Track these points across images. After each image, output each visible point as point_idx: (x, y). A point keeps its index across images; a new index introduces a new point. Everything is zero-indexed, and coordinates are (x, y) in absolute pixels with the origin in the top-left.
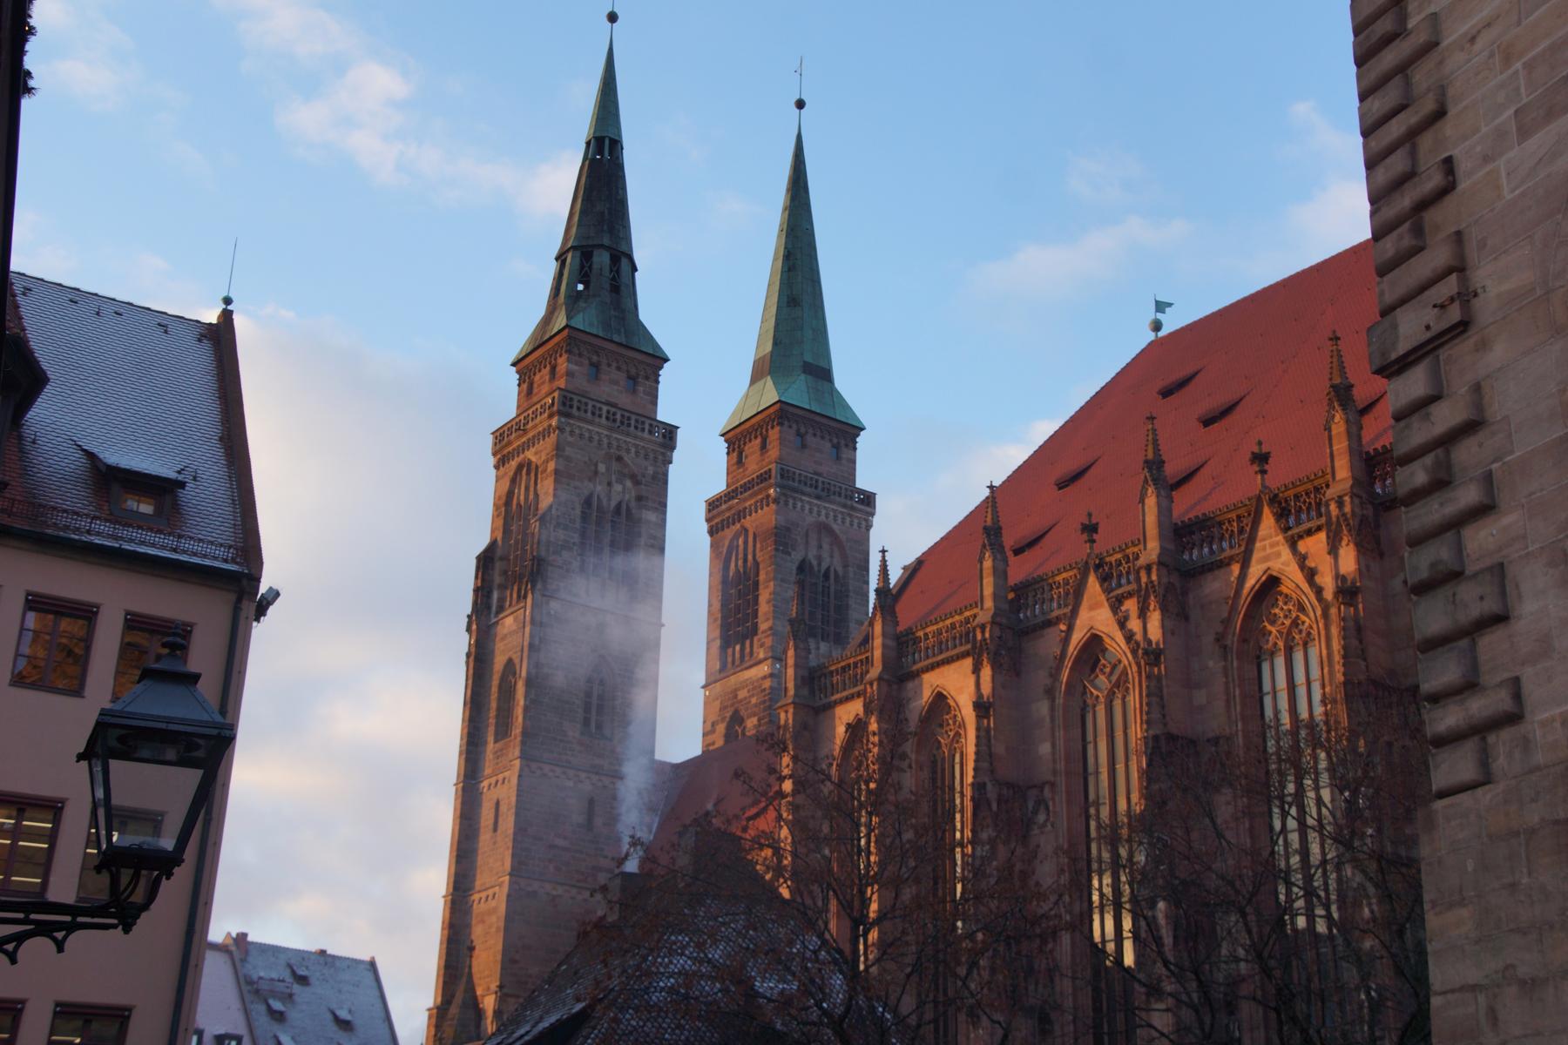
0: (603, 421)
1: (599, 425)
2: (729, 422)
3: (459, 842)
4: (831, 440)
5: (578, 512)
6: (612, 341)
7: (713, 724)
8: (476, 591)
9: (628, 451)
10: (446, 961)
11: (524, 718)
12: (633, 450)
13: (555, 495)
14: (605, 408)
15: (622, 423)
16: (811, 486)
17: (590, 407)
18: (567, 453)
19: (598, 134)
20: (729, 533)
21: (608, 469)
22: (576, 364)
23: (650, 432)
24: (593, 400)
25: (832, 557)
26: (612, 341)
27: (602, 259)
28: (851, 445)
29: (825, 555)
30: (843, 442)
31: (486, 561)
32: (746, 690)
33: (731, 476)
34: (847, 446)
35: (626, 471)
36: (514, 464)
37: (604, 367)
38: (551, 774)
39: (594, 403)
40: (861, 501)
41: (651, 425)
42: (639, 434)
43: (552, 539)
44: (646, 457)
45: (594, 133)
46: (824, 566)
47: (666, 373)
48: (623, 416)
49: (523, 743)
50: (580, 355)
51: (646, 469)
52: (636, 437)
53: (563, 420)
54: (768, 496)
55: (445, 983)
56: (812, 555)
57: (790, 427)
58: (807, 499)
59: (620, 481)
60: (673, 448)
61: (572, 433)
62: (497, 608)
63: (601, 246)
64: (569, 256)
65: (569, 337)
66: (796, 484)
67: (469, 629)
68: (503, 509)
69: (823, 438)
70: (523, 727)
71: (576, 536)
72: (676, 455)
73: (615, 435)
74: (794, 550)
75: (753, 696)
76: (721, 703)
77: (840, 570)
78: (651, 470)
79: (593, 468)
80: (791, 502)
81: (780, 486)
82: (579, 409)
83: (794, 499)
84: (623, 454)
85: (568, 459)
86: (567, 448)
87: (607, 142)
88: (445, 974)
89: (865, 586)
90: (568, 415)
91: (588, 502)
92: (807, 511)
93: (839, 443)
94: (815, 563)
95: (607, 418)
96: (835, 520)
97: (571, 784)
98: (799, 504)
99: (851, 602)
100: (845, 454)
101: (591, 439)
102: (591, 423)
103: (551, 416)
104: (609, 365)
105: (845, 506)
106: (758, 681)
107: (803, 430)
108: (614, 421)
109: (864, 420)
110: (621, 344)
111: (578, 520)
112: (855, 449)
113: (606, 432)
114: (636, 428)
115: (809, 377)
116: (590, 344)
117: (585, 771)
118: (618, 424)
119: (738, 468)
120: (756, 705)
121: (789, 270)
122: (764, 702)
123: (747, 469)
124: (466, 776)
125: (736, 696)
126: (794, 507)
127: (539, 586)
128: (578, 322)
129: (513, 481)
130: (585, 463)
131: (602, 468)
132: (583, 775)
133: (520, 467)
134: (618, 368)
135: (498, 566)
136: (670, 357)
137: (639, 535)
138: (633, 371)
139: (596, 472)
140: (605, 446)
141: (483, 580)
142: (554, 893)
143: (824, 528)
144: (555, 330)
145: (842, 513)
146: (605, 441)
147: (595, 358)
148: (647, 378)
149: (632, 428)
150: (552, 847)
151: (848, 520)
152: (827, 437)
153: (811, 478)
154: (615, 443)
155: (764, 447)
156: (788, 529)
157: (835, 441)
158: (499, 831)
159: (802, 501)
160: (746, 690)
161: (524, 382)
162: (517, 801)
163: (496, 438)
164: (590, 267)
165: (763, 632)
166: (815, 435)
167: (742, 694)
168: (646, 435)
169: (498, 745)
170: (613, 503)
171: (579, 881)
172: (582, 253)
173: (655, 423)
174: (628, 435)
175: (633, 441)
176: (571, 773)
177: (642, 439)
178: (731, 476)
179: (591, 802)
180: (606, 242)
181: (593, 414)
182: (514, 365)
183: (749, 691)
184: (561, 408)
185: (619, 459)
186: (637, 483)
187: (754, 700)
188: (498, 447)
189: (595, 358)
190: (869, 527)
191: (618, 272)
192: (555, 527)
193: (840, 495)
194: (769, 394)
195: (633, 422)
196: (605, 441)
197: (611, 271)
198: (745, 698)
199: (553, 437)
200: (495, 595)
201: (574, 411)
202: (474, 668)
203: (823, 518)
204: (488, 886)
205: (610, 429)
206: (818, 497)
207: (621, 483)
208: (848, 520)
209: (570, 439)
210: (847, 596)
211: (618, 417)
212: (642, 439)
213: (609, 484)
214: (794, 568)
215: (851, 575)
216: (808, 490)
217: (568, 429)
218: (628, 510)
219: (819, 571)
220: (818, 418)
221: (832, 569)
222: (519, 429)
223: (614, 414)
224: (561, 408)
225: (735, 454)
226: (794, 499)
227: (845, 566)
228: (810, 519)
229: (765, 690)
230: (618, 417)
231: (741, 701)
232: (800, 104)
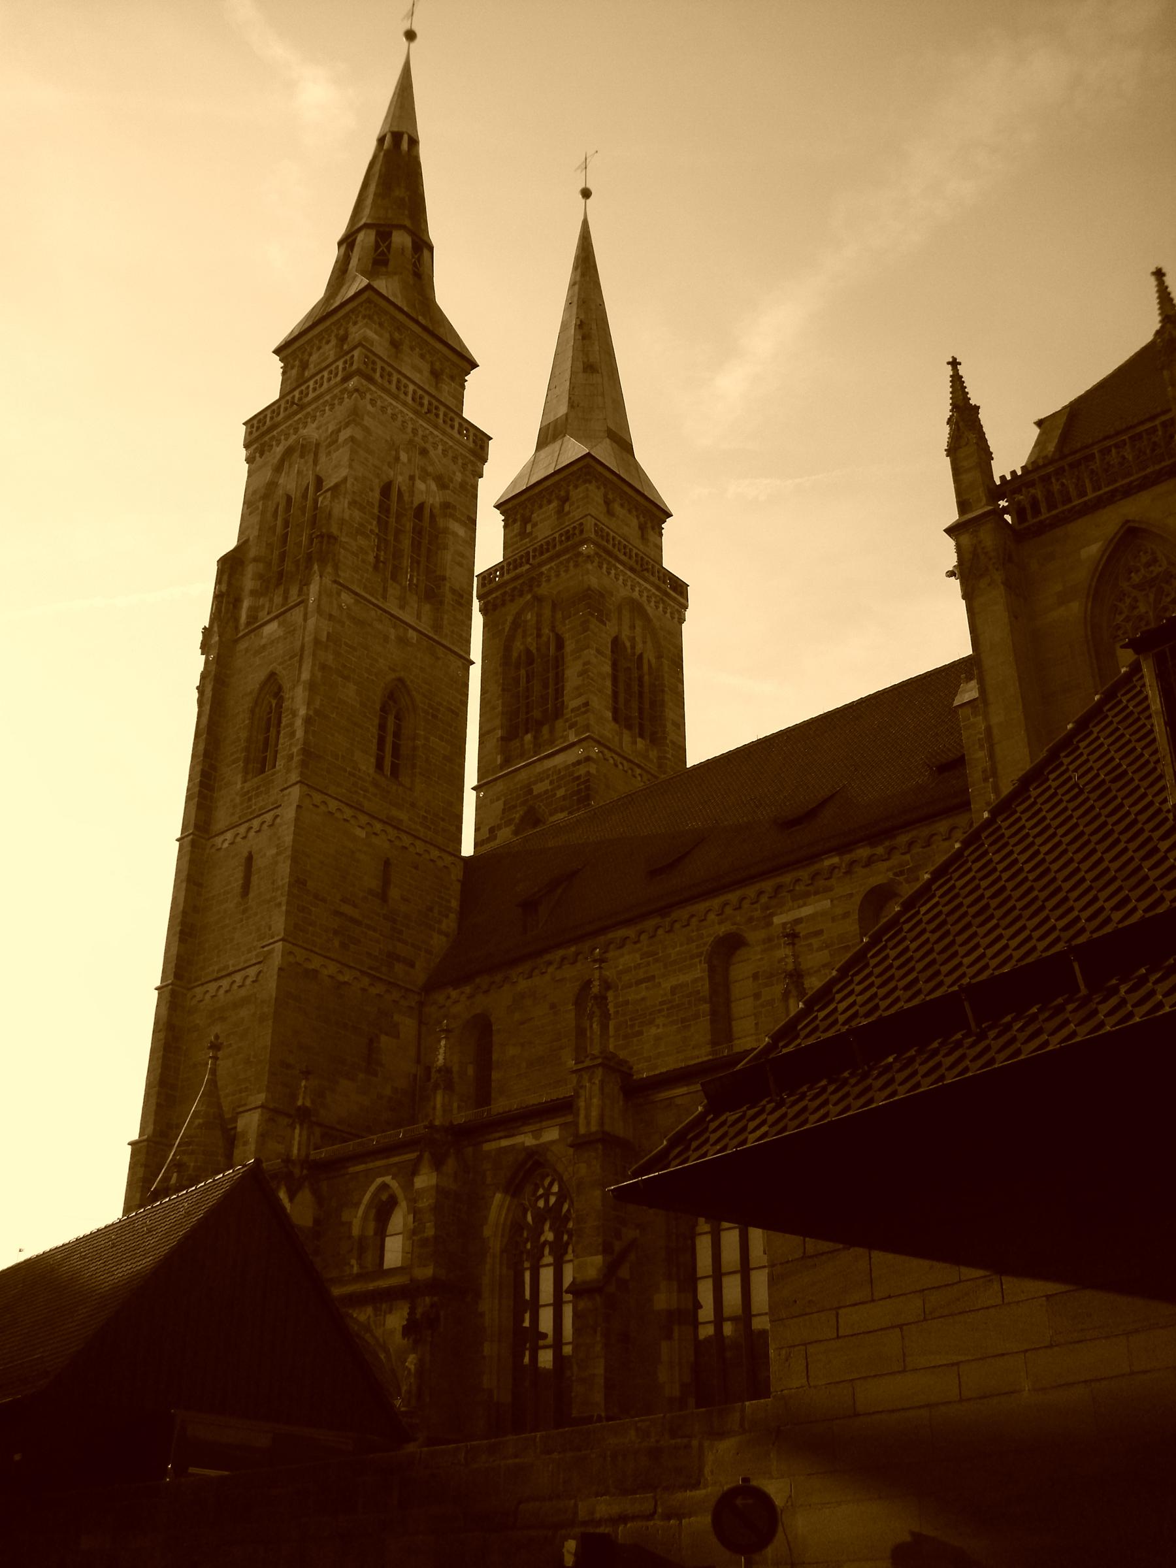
0: (409, 399)
1: (405, 404)
2: (514, 483)
3: (185, 913)
4: (638, 517)
5: (377, 495)
6: (417, 322)
7: (492, 830)
8: (218, 597)
9: (435, 448)
10: (162, 1074)
11: (306, 732)
12: (440, 447)
13: (350, 466)
14: (411, 387)
15: (429, 411)
16: (625, 554)
17: (394, 379)
18: (365, 423)
20: (512, 609)
21: (409, 460)
22: (376, 333)
23: (460, 433)
24: (399, 372)
25: (644, 643)
26: (417, 322)
27: (401, 239)
28: (657, 530)
29: (638, 639)
30: (649, 525)
31: (229, 566)
32: (547, 782)
33: (510, 550)
34: (653, 529)
35: (430, 469)
36: (279, 450)
37: (405, 348)
38: (338, 815)
39: (399, 376)
40: (674, 589)
41: (460, 425)
42: (449, 430)
43: (347, 516)
44: (454, 459)
45: (391, 125)
46: (638, 651)
47: (472, 379)
48: (430, 404)
49: (304, 764)
50: (381, 325)
51: (454, 473)
52: (444, 433)
53: (364, 382)
54: (580, 554)
55: (158, 1105)
56: (626, 633)
57: (598, 488)
58: (621, 568)
59: (423, 479)
60: (485, 460)
61: (373, 402)
62: (248, 617)
63: (401, 227)
64: (361, 236)
65: (369, 301)
66: (610, 547)
67: (205, 647)
68: (260, 504)
69: (630, 511)
70: (304, 744)
71: (375, 523)
72: (486, 467)
73: (421, 422)
74: (609, 621)
75: (559, 787)
76: (505, 804)
77: (653, 661)
78: (458, 477)
79: (394, 453)
80: (605, 566)
81: (595, 544)
82: (382, 376)
83: (609, 563)
84: (429, 447)
85: (367, 430)
86: (366, 417)
87: (406, 137)
88: (159, 1094)
89: (680, 685)
90: (370, 379)
91: (386, 490)
92: (621, 581)
93: (646, 523)
94: (628, 644)
95: (413, 399)
96: (649, 601)
97: (362, 834)
98: (613, 572)
99: (667, 697)
100: (652, 536)
101: (394, 417)
102: (396, 398)
103: (346, 379)
104: (412, 348)
105: (658, 588)
106: (567, 767)
107: (610, 496)
108: (422, 405)
109: (671, 506)
110: (425, 328)
111: (377, 505)
112: (661, 535)
113: (411, 415)
114: (444, 422)
115: (614, 445)
116: (393, 318)
117: (381, 821)
118: (425, 409)
119: (522, 540)
120: (564, 798)
121: (584, 338)
122: (579, 791)
123: (536, 537)
124: (196, 827)
125: (530, 791)
126: (609, 573)
127: (329, 569)
128: (381, 285)
129: (278, 469)
130: (386, 441)
131: (404, 457)
132: (378, 826)
133: (289, 452)
134: (422, 356)
135: (250, 570)
136: (478, 361)
137: (446, 548)
138: (438, 365)
139: (397, 459)
140: (409, 430)
141: (229, 584)
142: (341, 978)
143: (636, 608)
144: (351, 293)
145: (656, 596)
146: (410, 426)
147: (397, 335)
148: (452, 378)
149: (440, 421)
150: (338, 913)
151: (661, 606)
152: (635, 513)
153: (625, 547)
154: (420, 433)
155: (560, 512)
156: (602, 595)
157: (642, 519)
158: (251, 895)
159: (616, 568)
160: (547, 782)
161: (292, 368)
162: (294, 841)
163: (252, 426)
164: (389, 247)
165: (573, 710)
166: (622, 506)
167: (538, 789)
168: (455, 433)
169: (247, 785)
170: (416, 504)
171: (371, 968)
172: (379, 234)
173: (465, 425)
174: (436, 427)
175: (441, 436)
176: (364, 819)
177: (451, 437)
178: (510, 550)
179: (387, 863)
180: (408, 223)
181: (398, 388)
182: (277, 352)
183: (551, 783)
184: (363, 367)
185: (424, 452)
186: (443, 486)
187: (561, 793)
188: (255, 434)
189: (397, 335)
190: (682, 620)
191: (419, 259)
192: (350, 504)
193: (653, 574)
194: (573, 449)
195: (441, 416)
196: (410, 426)
197: (413, 257)
198: (546, 792)
199: (348, 402)
200: (246, 604)
201: (377, 376)
202: (213, 689)
203: (636, 595)
204: (231, 969)
205: (416, 412)
206: (632, 569)
207: (425, 482)
208: (661, 606)
209: (369, 408)
210: (663, 691)
211: (426, 402)
212: (451, 437)
213: (412, 478)
214: (610, 640)
215: (666, 668)
216: (622, 557)
217: (368, 396)
218: (432, 516)
219: (634, 654)
220: (626, 489)
221: (645, 656)
222: (293, 403)
223: (421, 398)
224: (363, 367)
225: (517, 525)
226: (609, 563)
227: (659, 657)
228: (624, 592)
229: (578, 778)
230: (426, 402)
231: (539, 796)
232: (586, 193)
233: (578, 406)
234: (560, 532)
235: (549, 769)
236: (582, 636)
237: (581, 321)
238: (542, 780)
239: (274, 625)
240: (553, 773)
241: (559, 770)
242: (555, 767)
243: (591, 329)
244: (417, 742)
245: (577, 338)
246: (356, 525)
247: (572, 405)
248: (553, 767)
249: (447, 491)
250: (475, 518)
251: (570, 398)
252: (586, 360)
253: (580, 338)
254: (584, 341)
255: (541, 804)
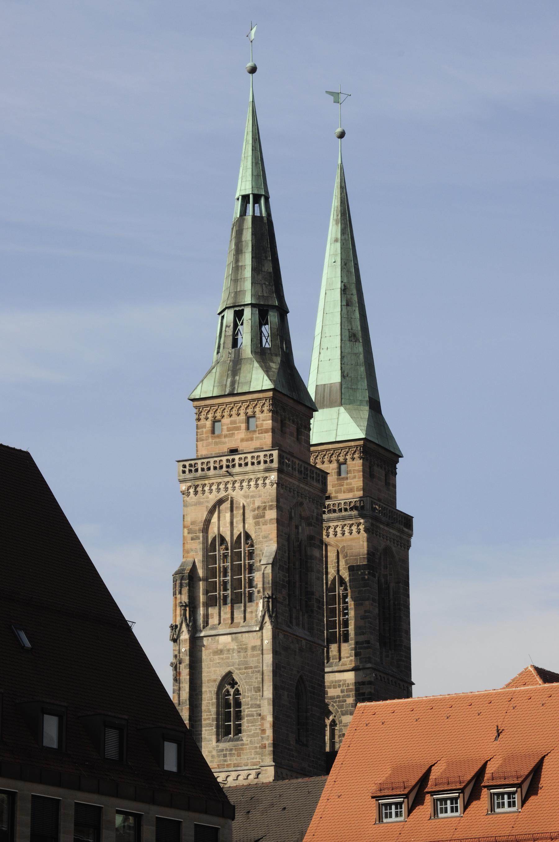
19: (256, 192)
32: (339, 690)
121: (347, 305)
160: (339, 690)
183: (342, 691)
190: (408, 546)
198: (338, 697)
233: (347, 376)
234: (345, 501)
235: (341, 681)
236: (364, 589)
237: (345, 286)
238: (335, 687)
239: (228, 638)
240: (343, 685)
241: (348, 684)
242: (345, 680)
243: (352, 294)
244: (308, 714)
245: (343, 304)
246: (281, 583)
247: (343, 376)
248: (343, 680)
249: (311, 528)
250: (280, 475)
251: (341, 368)
252: (350, 328)
253: (345, 304)
254: (349, 308)
255: (335, 704)
